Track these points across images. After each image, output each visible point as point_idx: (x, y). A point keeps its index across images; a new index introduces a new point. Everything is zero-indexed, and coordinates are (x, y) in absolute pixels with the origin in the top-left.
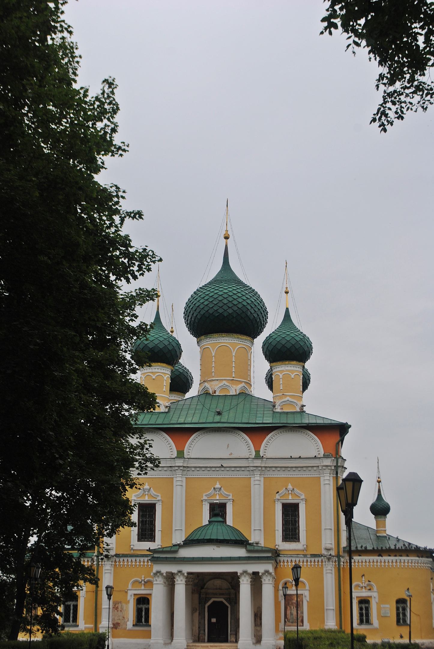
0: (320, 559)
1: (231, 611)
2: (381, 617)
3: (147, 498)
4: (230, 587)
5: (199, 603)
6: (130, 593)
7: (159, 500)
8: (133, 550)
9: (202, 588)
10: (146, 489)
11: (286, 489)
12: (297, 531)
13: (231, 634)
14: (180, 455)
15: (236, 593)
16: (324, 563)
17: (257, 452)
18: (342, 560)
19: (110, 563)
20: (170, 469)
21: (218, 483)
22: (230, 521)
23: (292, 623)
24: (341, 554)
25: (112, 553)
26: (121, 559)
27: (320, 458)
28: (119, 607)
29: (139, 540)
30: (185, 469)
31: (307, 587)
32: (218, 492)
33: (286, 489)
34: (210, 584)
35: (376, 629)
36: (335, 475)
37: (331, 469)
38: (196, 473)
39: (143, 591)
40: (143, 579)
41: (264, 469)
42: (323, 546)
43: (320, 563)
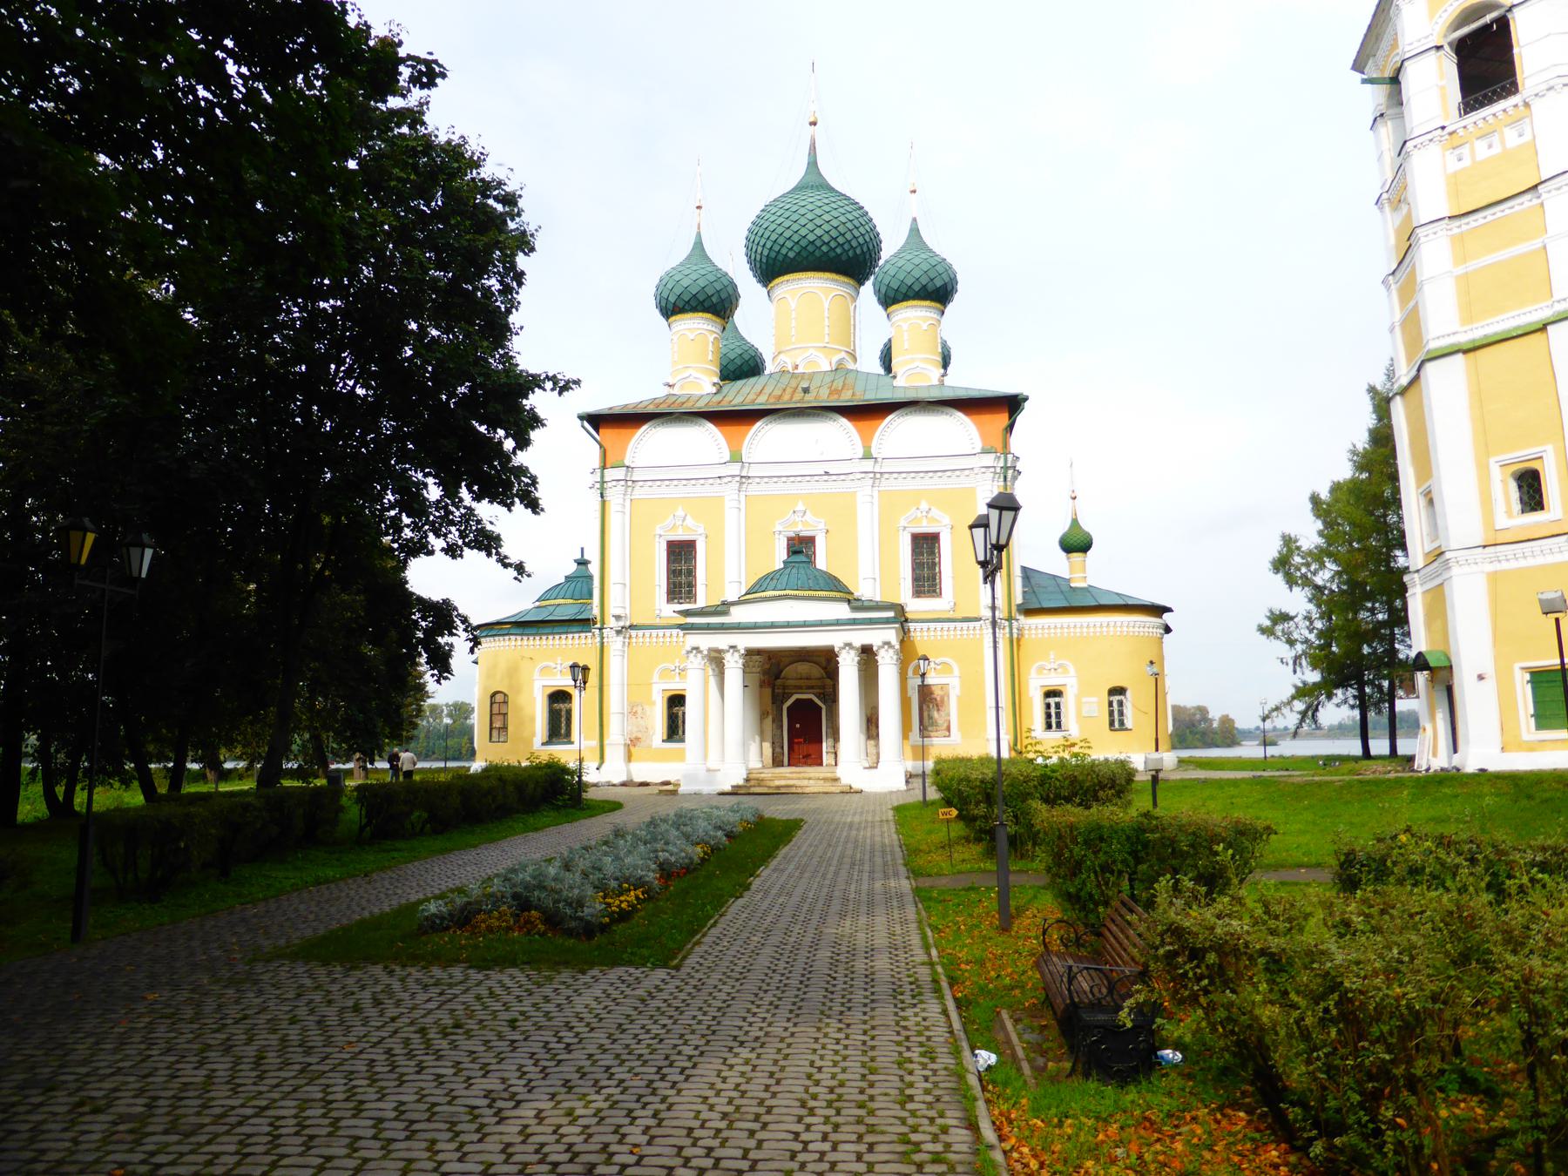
0: (977, 624)
3: (680, 531)
9: (777, 677)
14: (736, 458)
18: (1015, 624)
20: (718, 481)
22: (821, 563)
31: (956, 672)
34: (789, 671)
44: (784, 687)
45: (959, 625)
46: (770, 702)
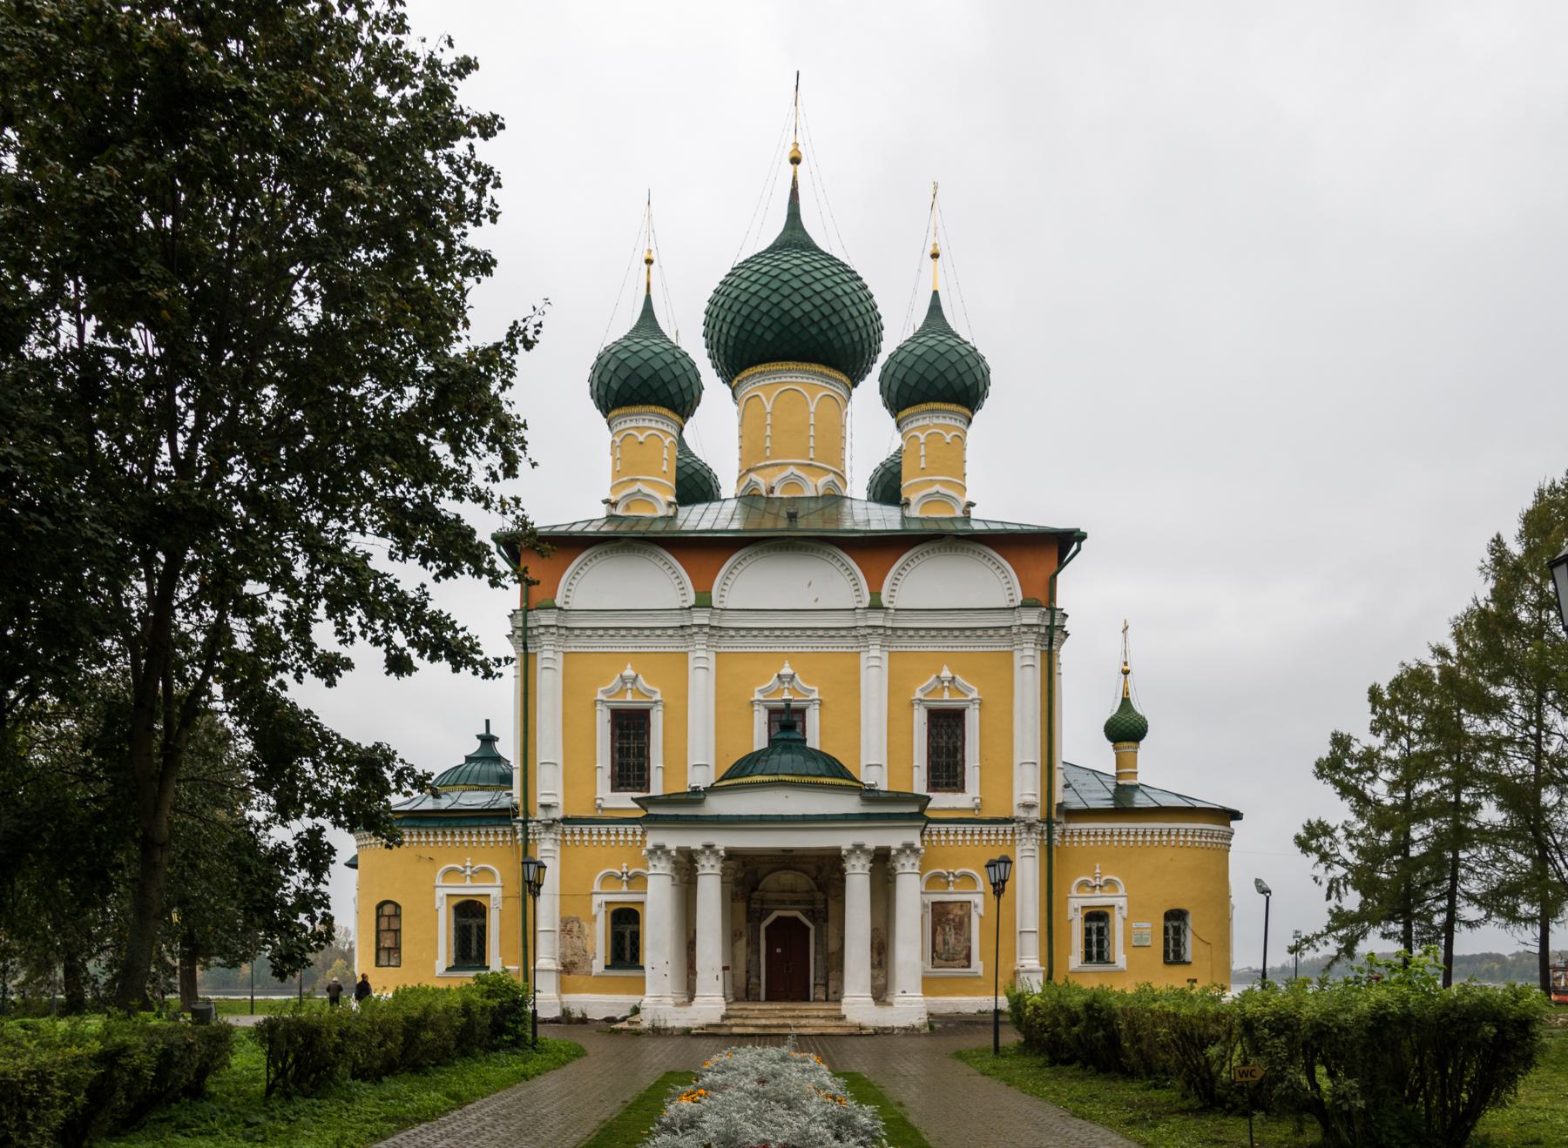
0: (1009, 828)
1: (816, 937)
2: (1133, 947)
3: (629, 697)
4: (815, 888)
5: (748, 921)
6: (597, 899)
7: (656, 702)
8: (603, 809)
9: (754, 889)
10: (628, 678)
11: (938, 677)
12: (959, 770)
13: (815, 985)
14: (703, 602)
15: (826, 900)
16: (1017, 837)
17: (875, 594)
18: (1057, 829)
19: (553, 836)
20: (680, 632)
21: (787, 665)
23: (946, 960)
24: (1054, 816)
25: (557, 814)
26: (577, 829)
27: (1014, 608)
28: (575, 929)
29: (614, 789)
30: (714, 632)
31: (981, 888)
32: (786, 685)
33: (938, 677)
34: (770, 882)
35: (1121, 971)
36: (1045, 648)
37: (1039, 634)
38: (739, 641)
39: (624, 896)
40: (625, 870)
41: (889, 632)
42: (1017, 800)
43: (1009, 837)
44: (763, 902)
45: (985, 828)
46: (742, 918)
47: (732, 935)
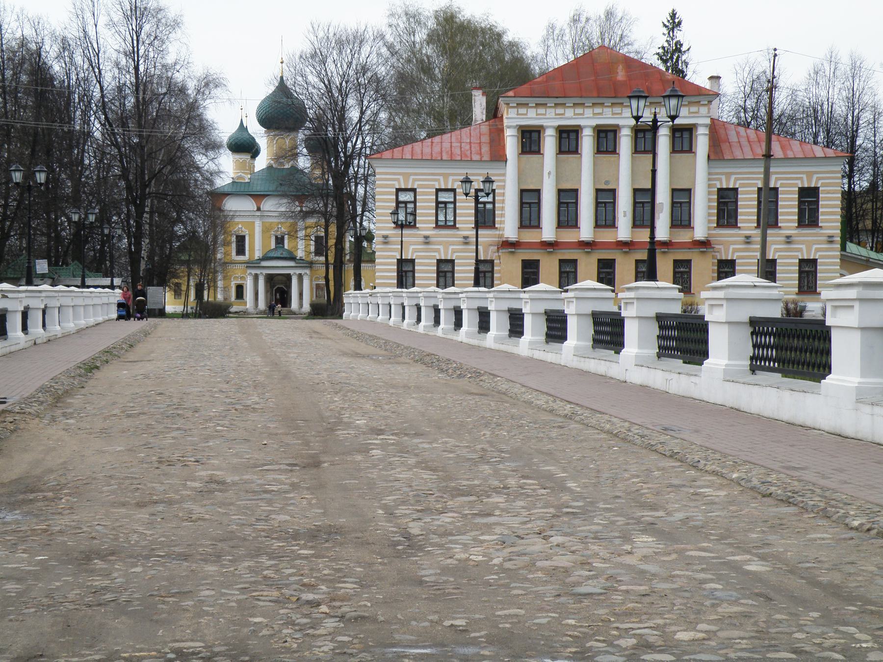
14: (259, 209)
22: (286, 247)
34: (276, 278)
39: (239, 282)
47: (267, 292)
